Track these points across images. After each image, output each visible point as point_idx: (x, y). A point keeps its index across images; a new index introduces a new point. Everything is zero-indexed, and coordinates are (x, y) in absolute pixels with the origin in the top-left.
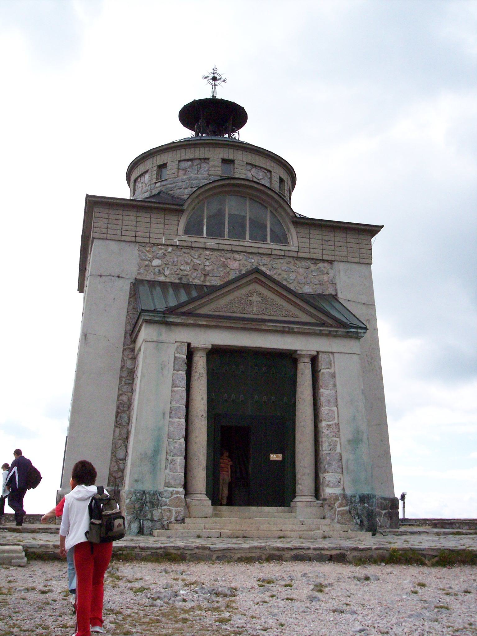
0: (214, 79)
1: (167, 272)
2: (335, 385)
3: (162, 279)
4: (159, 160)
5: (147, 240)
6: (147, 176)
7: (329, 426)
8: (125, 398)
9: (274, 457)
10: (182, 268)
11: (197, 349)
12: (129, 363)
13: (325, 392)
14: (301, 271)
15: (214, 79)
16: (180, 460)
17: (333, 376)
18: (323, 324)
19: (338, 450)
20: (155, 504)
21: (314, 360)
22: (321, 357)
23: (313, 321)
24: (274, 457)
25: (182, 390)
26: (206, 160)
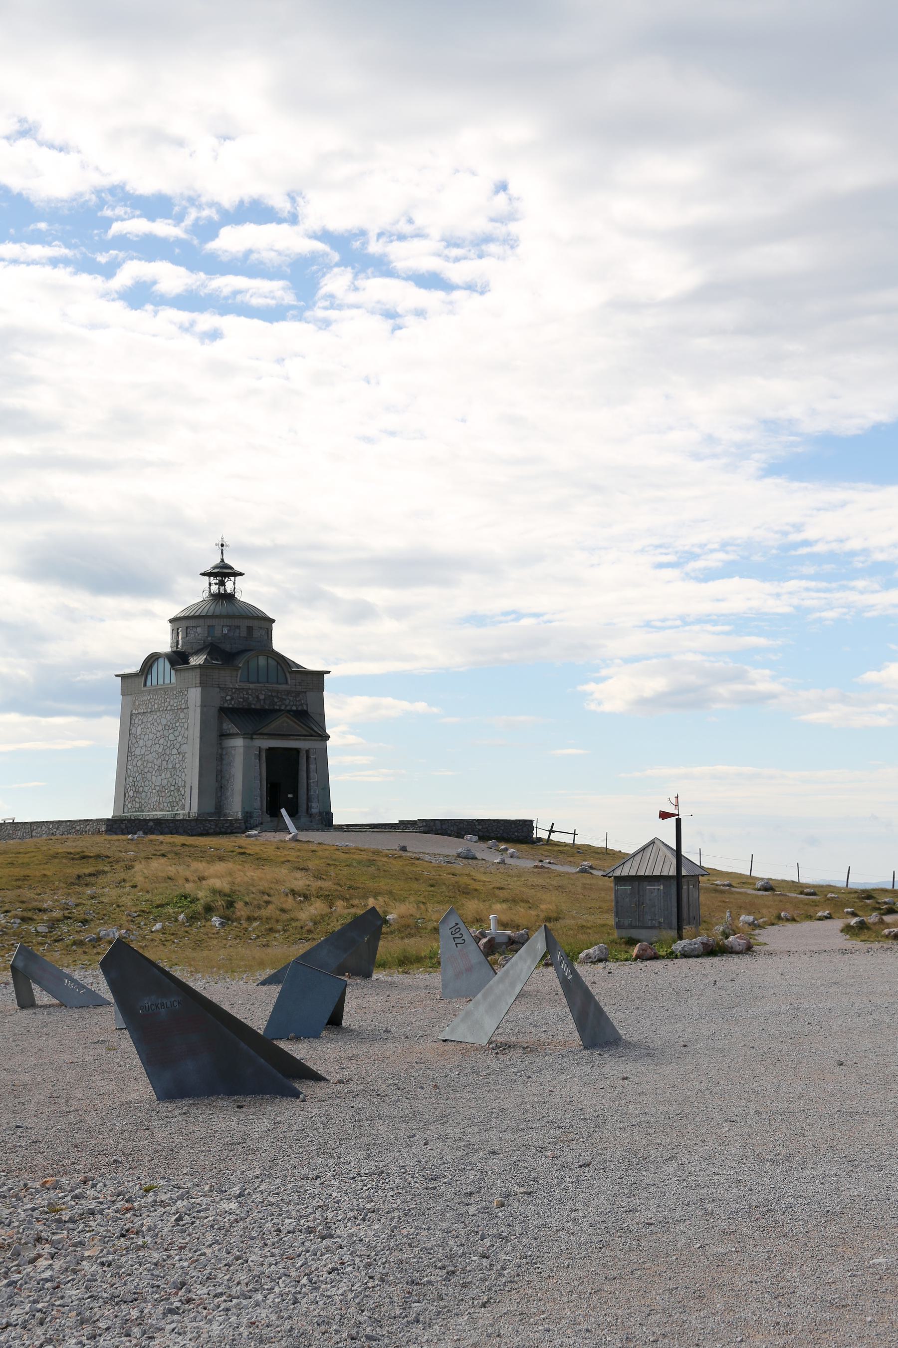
0: (222, 545)
1: (233, 703)
2: (316, 763)
3: (231, 706)
4: (209, 622)
5: (224, 686)
6: (199, 630)
7: (313, 782)
8: (219, 768)
9: (290, 796)
10: (239, 700)
11: (263, 749)
12: (220, 751)
13: (312, 767)
14: (291, 698)
15: (222, 545)
16: (259, 799)
17: (315, 759)
18: (312, 736)
19: (317, 792)
20: (251, 817)
21: (307, 752)
22: (311, 751)
23: (307, 734)
24: (290, 796)
25: (258, 767)
26: (238, 627)
